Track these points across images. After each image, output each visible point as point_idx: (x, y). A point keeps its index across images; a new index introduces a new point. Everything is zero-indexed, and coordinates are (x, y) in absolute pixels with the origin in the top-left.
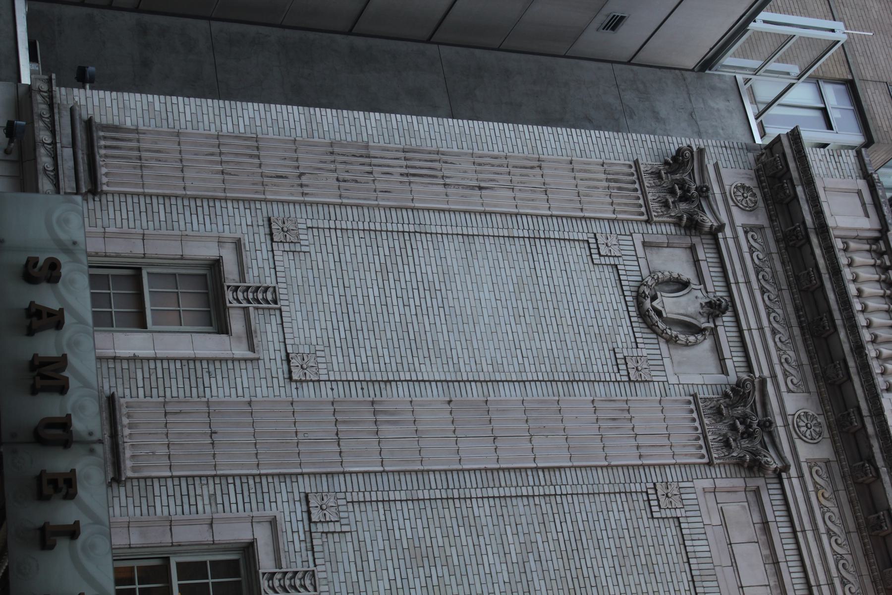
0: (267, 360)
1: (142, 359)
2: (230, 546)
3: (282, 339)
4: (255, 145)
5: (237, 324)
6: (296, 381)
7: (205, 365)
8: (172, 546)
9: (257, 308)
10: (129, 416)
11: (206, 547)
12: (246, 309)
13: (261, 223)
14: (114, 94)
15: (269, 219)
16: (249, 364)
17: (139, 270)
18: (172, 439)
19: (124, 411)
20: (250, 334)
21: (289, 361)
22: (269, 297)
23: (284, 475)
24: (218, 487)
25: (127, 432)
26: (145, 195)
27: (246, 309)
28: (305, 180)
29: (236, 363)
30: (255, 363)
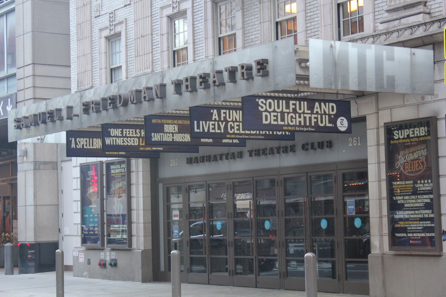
0: (126, 15)
1: (127, 67)
2: (170, 26)
3: (121, 9)
4: (79, 25)
5: (118, 29)
6: (130, 2)
7: (128, 41)
8: (168, 50)
9: (114, 21)
10: (138, 72)
11: (170, 36)
12: (115, 26)
13: (96, 21)
14: (72, 84)
15: (96, 17)
16: (128, 22)
17: (111, 69)
18: (143, 54)
19: (137, 73)
20: (121, 23)
21: (125, 6)
22: (111, 16)
23: (151, 4)
24: (155, 33)
25: (142, 72)
26: (92, 70)
27: (115, 25)
28: (85, 4)
29: (128, 28)
30: (127, 20)
